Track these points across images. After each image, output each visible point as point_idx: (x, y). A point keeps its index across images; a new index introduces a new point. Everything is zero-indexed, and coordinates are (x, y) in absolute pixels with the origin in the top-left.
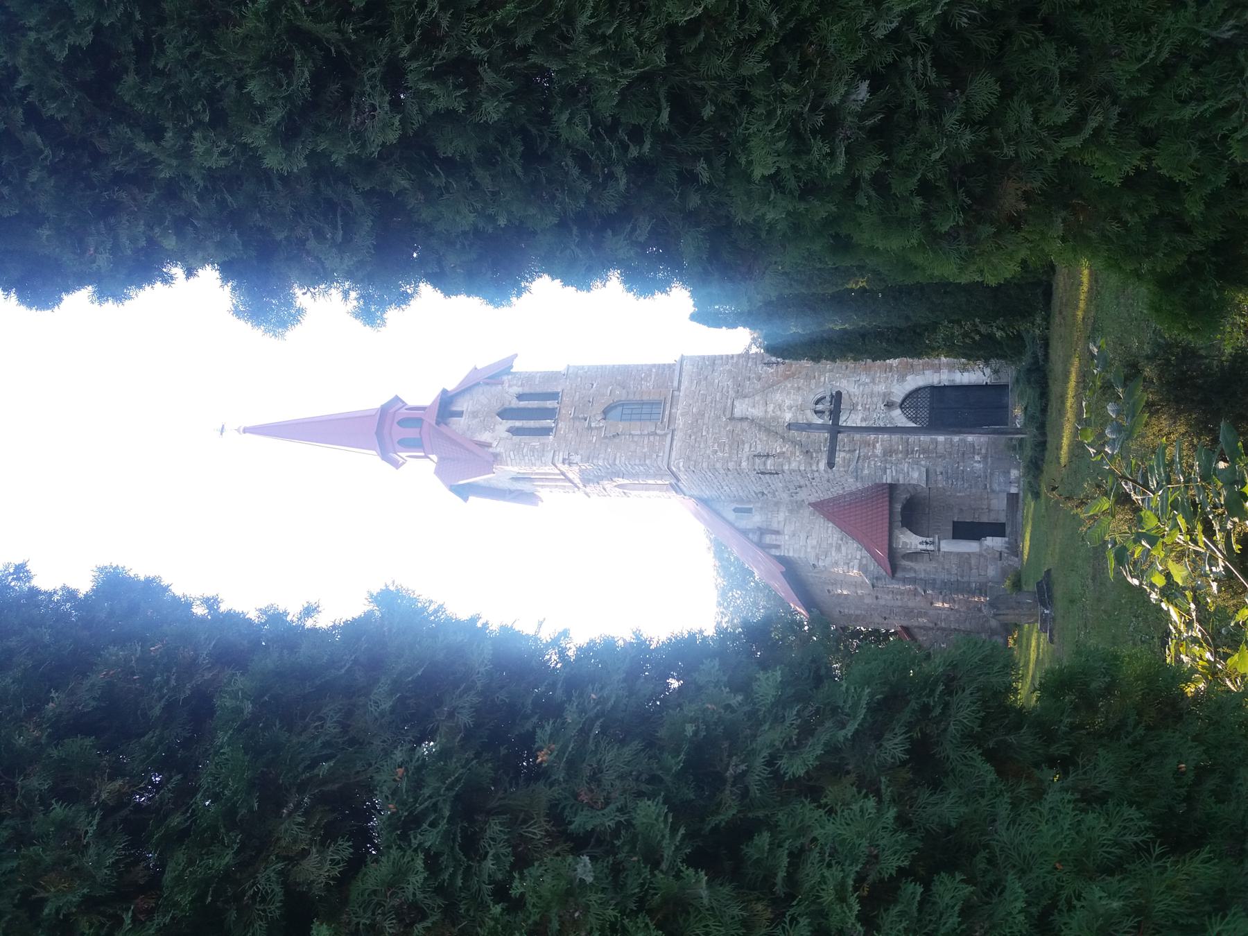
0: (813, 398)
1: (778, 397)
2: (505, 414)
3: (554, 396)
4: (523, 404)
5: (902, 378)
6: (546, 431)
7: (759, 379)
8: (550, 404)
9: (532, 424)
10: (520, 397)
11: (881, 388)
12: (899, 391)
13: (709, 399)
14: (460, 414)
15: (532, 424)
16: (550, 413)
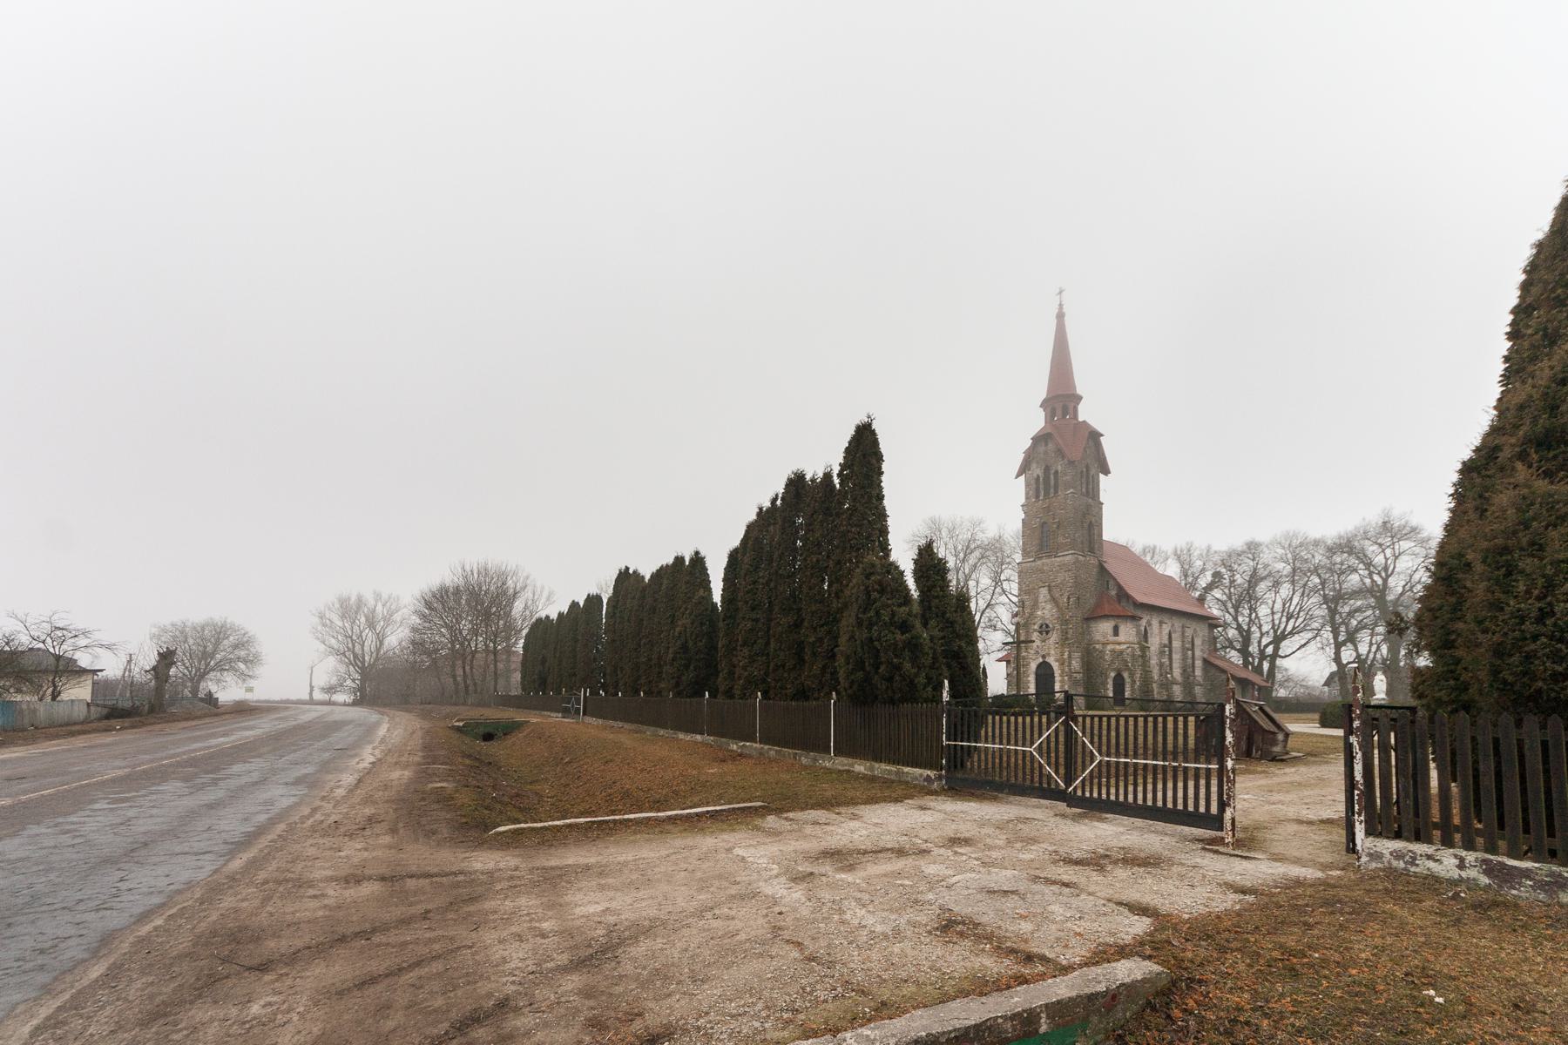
0: (1047, 622)
1: (1049, 606)
2: (1047, 470)
3: (1056, 492)
4: (1052, 477)
5: (1057, 660)
6: (1037, 497)
7: (1061, 595)
8: (1052, 490)
9: (1042, 486)
10: (1056, 472)
11: (1052, 652)
12: (1051, 660)
13: (1050, 573)
14: (1046, 445)
15: (1042, 486)
16: (1047, 494)
